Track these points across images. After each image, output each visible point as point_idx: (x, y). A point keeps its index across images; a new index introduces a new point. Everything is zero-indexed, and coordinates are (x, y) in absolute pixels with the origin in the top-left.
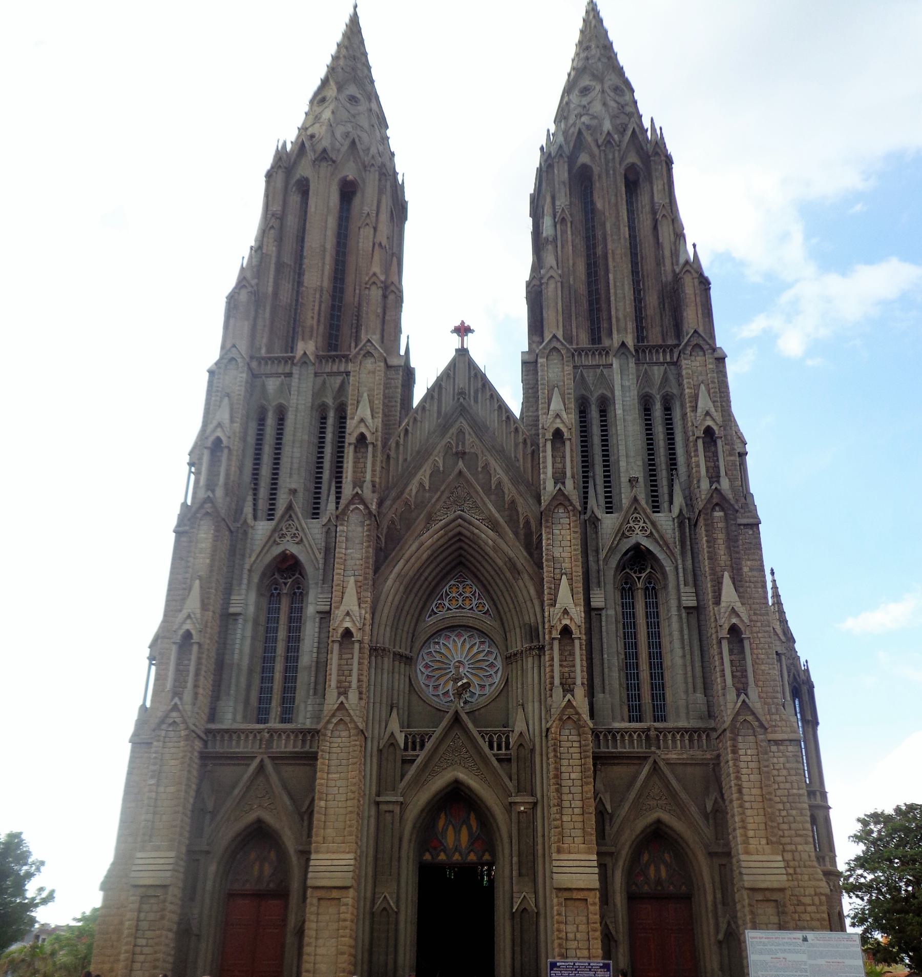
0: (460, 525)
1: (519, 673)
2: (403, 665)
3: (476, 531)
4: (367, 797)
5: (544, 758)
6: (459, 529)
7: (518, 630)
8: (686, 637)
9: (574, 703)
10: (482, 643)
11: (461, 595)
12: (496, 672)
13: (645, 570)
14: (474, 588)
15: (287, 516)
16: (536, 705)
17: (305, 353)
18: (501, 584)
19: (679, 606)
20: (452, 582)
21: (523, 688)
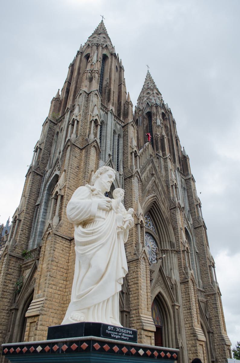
0: (156, 199)
1: (169, 257)
6: (155, 200)
7: (167, 242)
8: (197, 261)
15: (109, 164)
16: (177, 271)
17: (112, 110)
19: (194, 251)
20: (146, 216)
21: (171, 263)
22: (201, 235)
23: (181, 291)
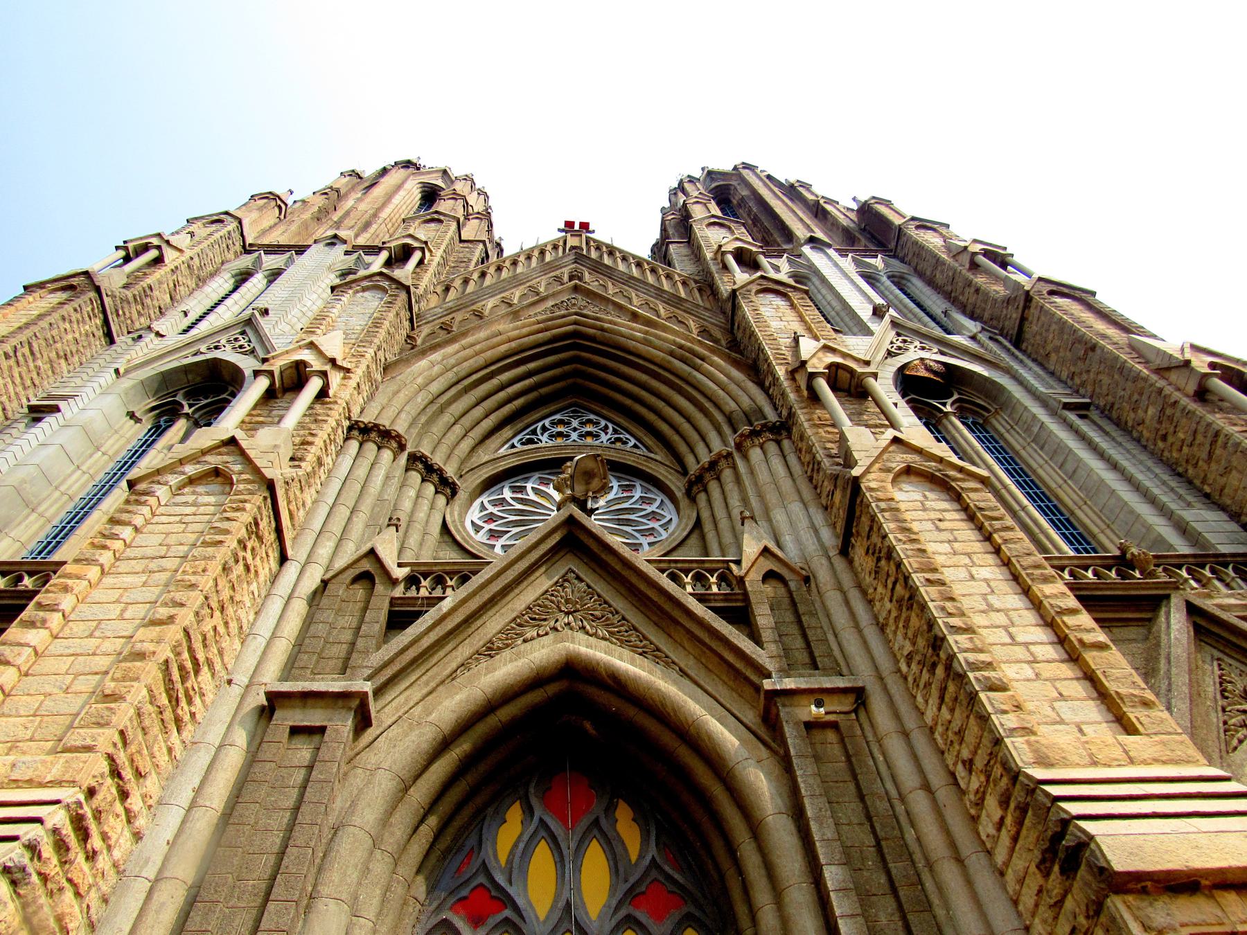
0: (576, 323)
2: (430, 489)
3: (606, 325)
4: (236, 691)
5: (854, 595)
9: (913, 442)
10: (629, 488)
11: (575, 430)
12: (665, 526)
13: (952, 396)
14: (603, 423)
16: (796, 507)
18: (664, 389)
19: (1053, 413)
20: (558, 417)
22: (1054, 327)
23: (864, 593)
